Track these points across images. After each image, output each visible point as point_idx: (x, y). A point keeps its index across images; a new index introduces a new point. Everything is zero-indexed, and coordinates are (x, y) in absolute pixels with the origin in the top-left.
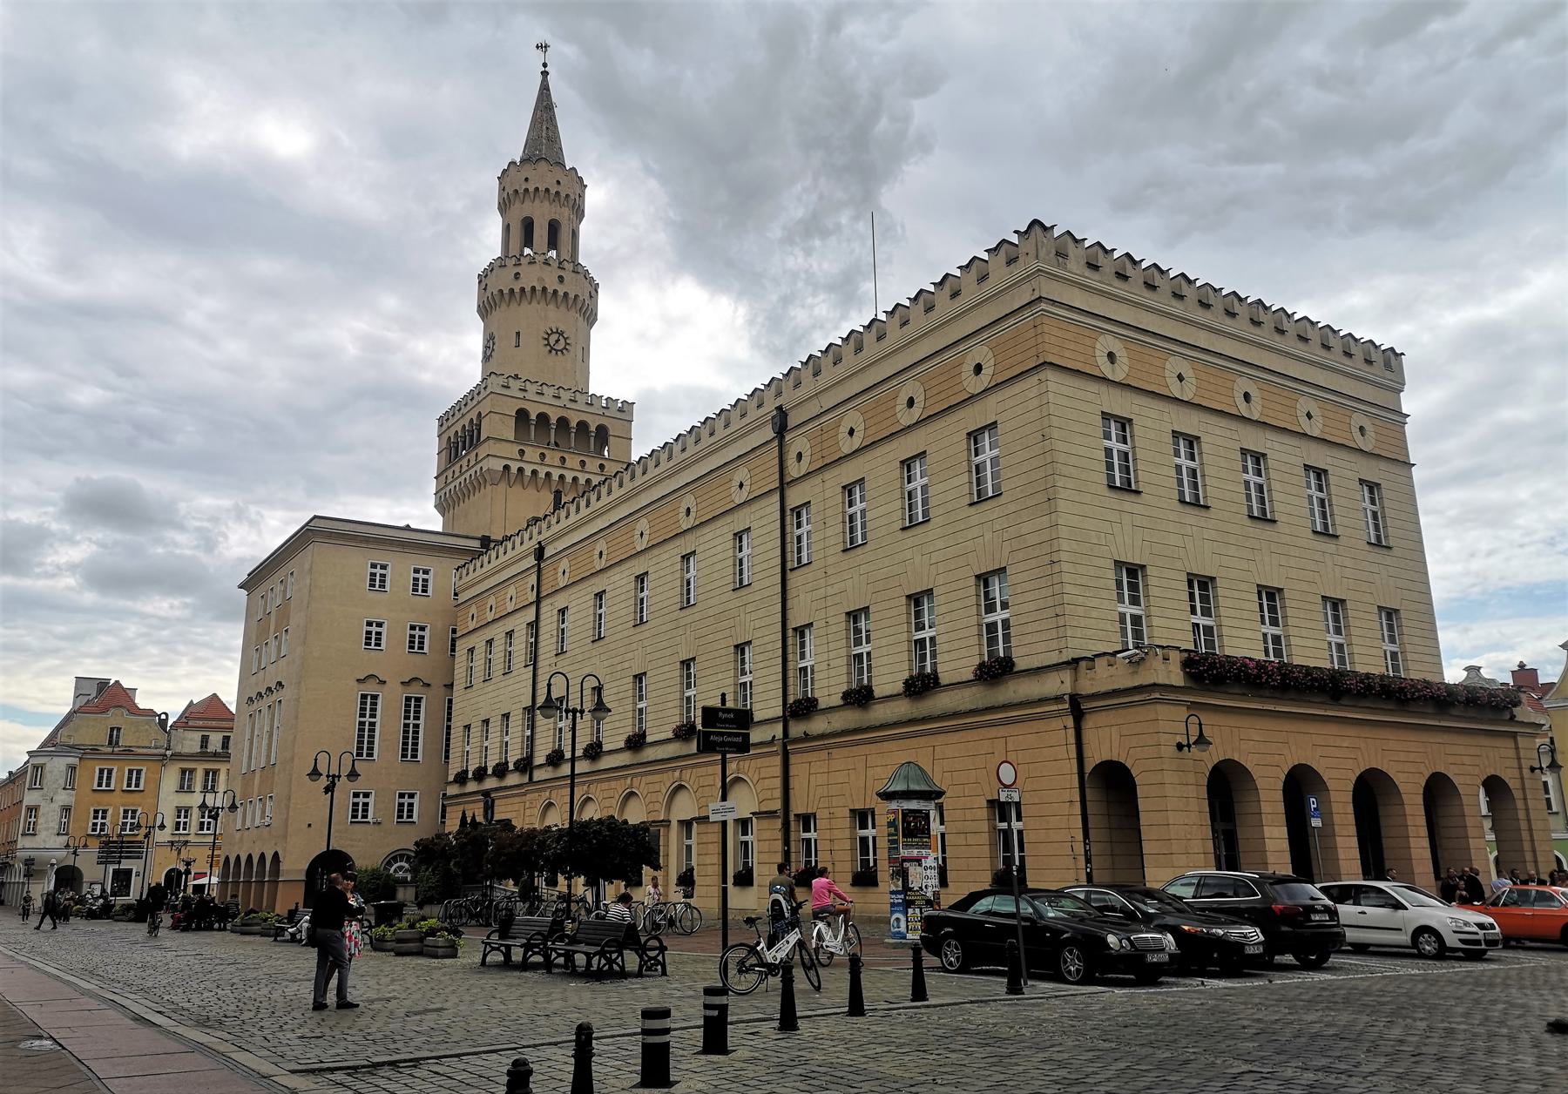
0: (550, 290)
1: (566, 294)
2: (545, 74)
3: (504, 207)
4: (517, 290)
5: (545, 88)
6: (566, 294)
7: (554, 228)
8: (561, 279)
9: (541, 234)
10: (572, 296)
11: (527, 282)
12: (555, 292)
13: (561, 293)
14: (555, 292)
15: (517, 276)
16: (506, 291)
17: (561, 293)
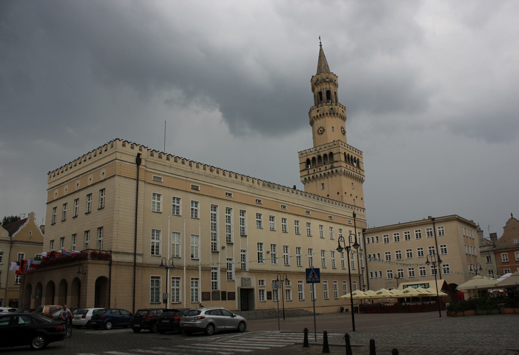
2: (321, 45)
3: (313, 90)
4: (318, 115)
5: (321, 50)
7: (328, 93)
8: (332, 109)
9: (324, 96)
11: (321, 112)
15: (318, 111)
16: (316, 116)
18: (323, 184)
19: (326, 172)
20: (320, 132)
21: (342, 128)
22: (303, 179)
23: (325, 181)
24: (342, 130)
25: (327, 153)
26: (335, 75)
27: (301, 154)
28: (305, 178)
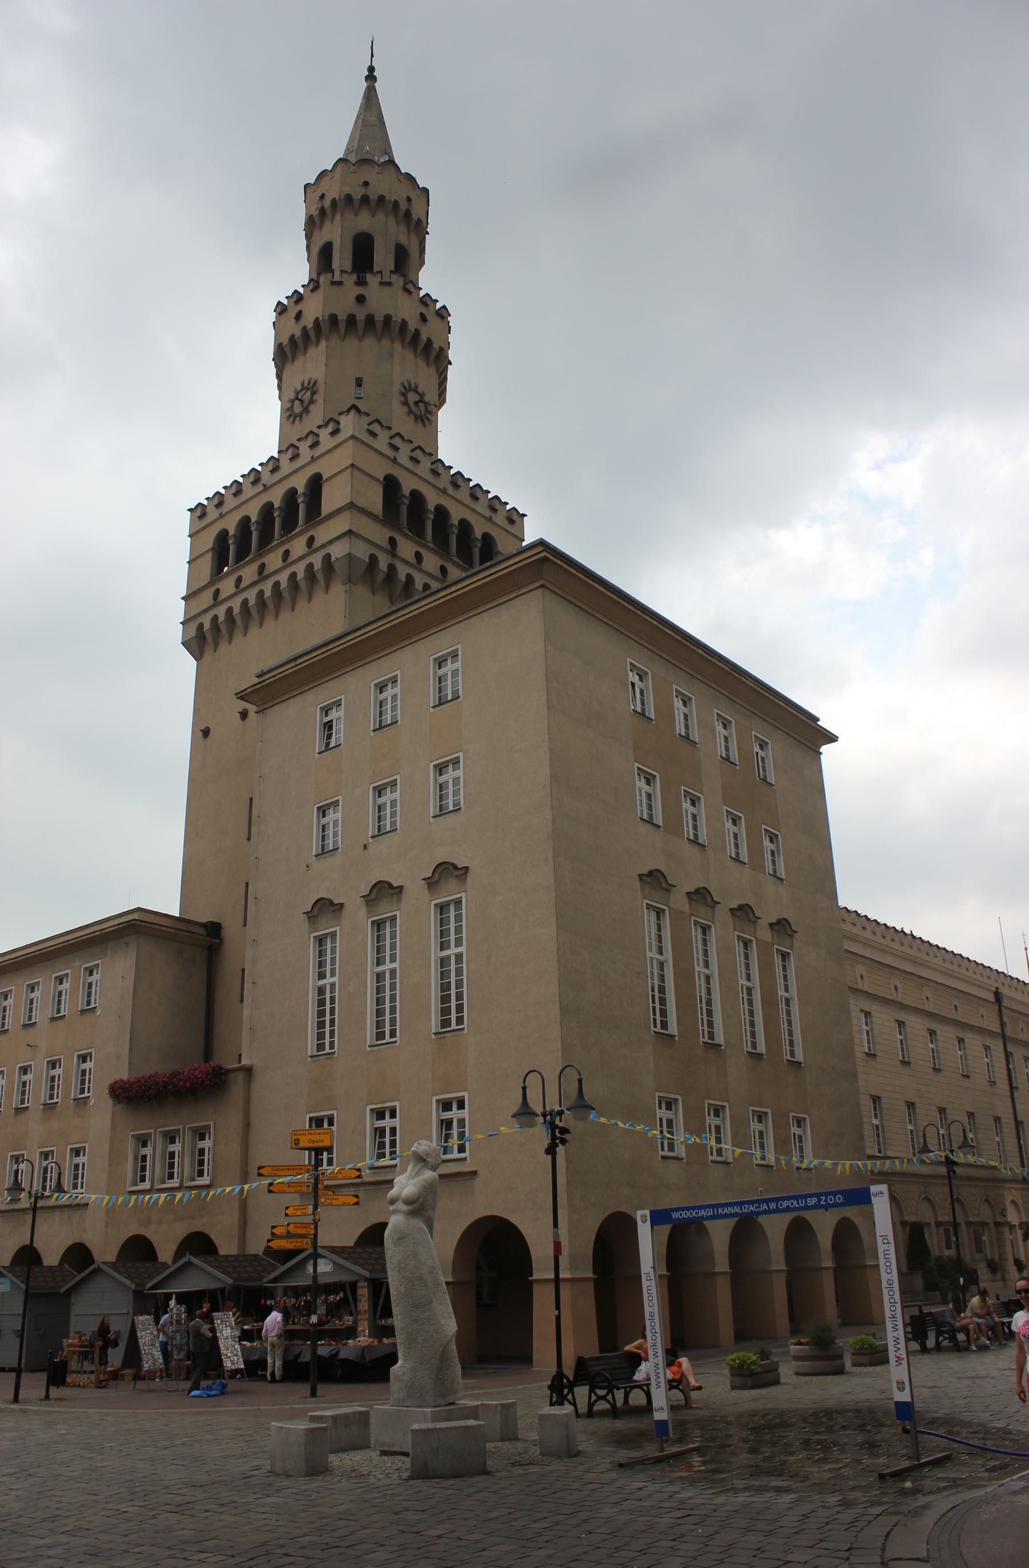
0: (342, 317)
1: (370, 320)
2: (371, 76)
5: (371, 98)
6: (370, 320)
8: (361, 299)
10: (379, 317)
11: (308, 321)
13: (361, 317)
14: (351, 320)
15: (299, 316)
17: (361, 317)
22: (192, 632)
24: (412, 397)
25: (300, 483)
26: (410, 178)
27: (199, 512)
28: (201, 626)
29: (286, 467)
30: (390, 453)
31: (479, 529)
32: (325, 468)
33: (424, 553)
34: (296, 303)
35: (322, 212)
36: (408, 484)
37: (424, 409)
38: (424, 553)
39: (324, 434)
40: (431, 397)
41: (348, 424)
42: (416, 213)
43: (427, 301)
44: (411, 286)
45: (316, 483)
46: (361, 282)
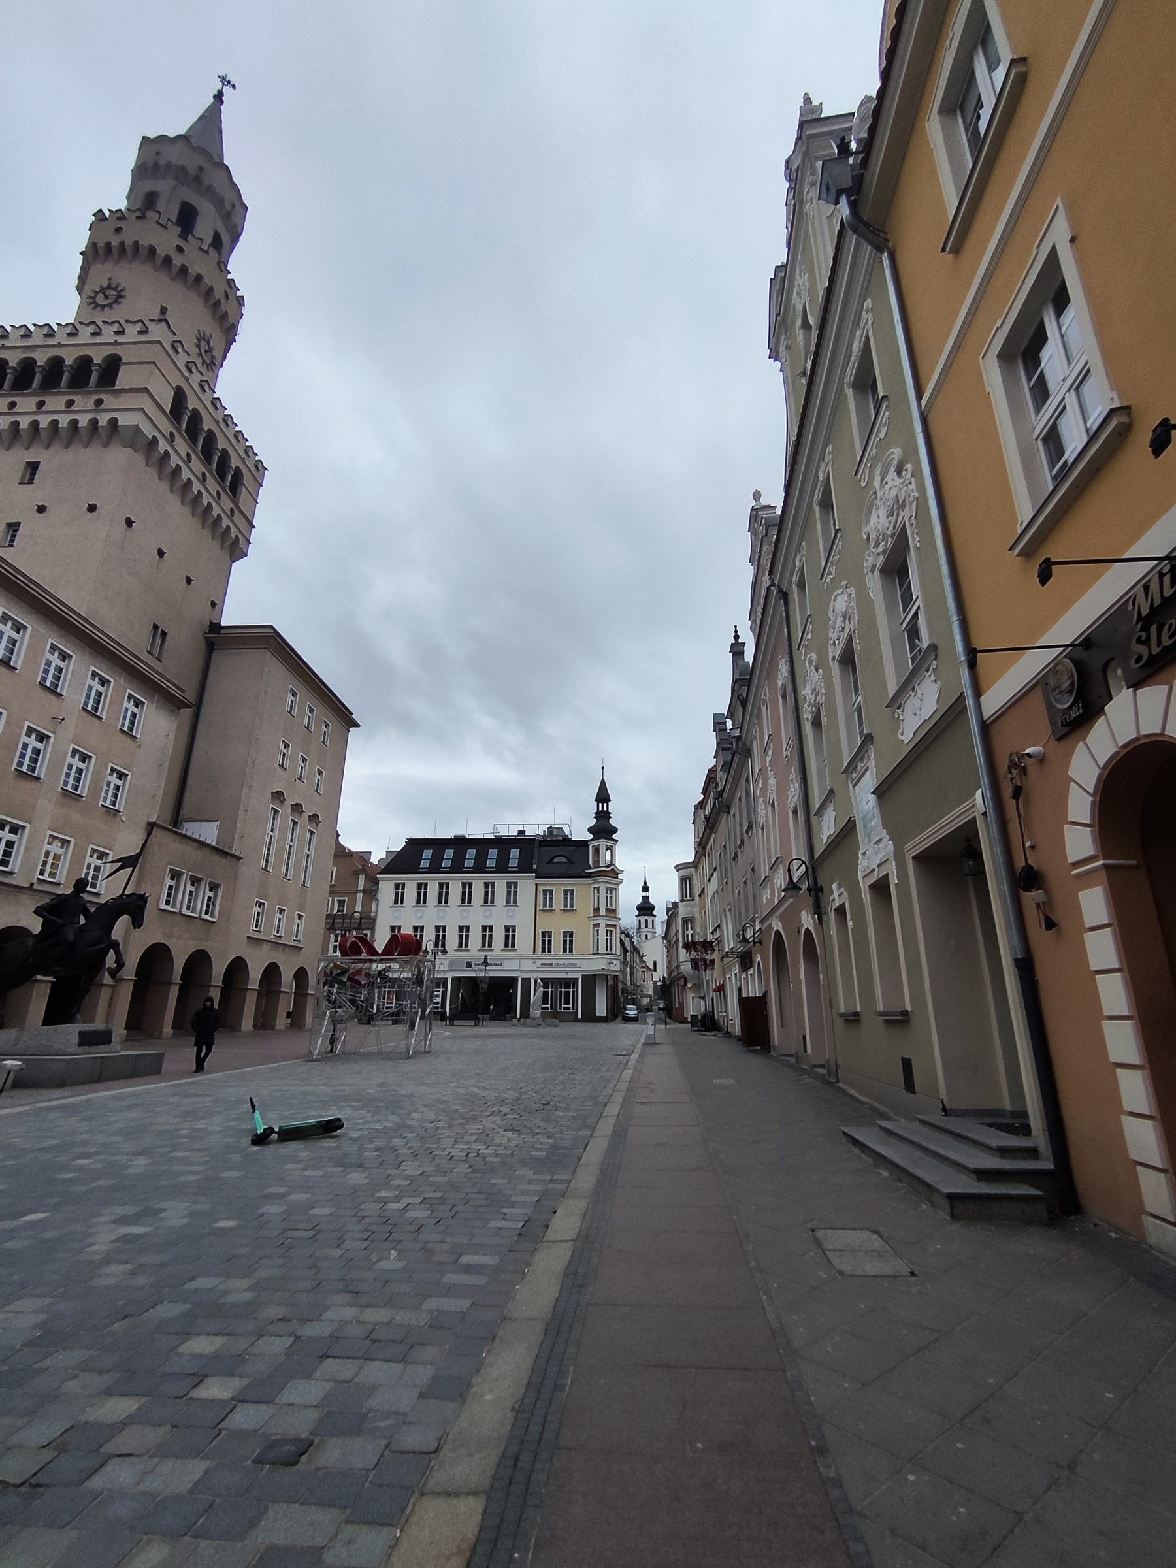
2: (219, 97)
11: (128, 238)
12: (168, 260)
15: (118, 230)
18: (33, 467)
19: (64, 421)
20: (100, 299)
21: (202, 338)
23: (50, 459)
29: (85, 335)
30: (186, 374)
31: (235, 462)
32: (125, 354)
33: (193, 456)
34: (118, 219)
35: (156, 166)
36: (192, 403)
37: (211, 359)
38: (193, 456)
39: (132, 331)
40: (217, 353)
41: (157, 332)
42: (235, 219)
43: (231, 283)
44: (222, 266)
45: (113, 365)
46: (184, 235)
